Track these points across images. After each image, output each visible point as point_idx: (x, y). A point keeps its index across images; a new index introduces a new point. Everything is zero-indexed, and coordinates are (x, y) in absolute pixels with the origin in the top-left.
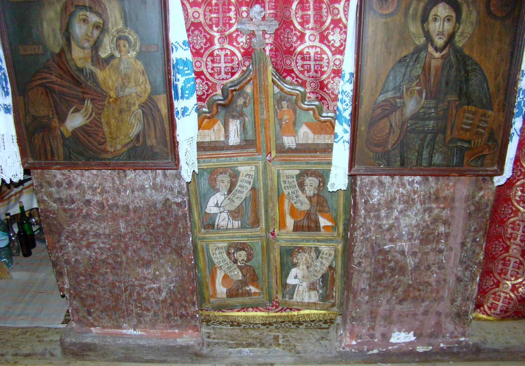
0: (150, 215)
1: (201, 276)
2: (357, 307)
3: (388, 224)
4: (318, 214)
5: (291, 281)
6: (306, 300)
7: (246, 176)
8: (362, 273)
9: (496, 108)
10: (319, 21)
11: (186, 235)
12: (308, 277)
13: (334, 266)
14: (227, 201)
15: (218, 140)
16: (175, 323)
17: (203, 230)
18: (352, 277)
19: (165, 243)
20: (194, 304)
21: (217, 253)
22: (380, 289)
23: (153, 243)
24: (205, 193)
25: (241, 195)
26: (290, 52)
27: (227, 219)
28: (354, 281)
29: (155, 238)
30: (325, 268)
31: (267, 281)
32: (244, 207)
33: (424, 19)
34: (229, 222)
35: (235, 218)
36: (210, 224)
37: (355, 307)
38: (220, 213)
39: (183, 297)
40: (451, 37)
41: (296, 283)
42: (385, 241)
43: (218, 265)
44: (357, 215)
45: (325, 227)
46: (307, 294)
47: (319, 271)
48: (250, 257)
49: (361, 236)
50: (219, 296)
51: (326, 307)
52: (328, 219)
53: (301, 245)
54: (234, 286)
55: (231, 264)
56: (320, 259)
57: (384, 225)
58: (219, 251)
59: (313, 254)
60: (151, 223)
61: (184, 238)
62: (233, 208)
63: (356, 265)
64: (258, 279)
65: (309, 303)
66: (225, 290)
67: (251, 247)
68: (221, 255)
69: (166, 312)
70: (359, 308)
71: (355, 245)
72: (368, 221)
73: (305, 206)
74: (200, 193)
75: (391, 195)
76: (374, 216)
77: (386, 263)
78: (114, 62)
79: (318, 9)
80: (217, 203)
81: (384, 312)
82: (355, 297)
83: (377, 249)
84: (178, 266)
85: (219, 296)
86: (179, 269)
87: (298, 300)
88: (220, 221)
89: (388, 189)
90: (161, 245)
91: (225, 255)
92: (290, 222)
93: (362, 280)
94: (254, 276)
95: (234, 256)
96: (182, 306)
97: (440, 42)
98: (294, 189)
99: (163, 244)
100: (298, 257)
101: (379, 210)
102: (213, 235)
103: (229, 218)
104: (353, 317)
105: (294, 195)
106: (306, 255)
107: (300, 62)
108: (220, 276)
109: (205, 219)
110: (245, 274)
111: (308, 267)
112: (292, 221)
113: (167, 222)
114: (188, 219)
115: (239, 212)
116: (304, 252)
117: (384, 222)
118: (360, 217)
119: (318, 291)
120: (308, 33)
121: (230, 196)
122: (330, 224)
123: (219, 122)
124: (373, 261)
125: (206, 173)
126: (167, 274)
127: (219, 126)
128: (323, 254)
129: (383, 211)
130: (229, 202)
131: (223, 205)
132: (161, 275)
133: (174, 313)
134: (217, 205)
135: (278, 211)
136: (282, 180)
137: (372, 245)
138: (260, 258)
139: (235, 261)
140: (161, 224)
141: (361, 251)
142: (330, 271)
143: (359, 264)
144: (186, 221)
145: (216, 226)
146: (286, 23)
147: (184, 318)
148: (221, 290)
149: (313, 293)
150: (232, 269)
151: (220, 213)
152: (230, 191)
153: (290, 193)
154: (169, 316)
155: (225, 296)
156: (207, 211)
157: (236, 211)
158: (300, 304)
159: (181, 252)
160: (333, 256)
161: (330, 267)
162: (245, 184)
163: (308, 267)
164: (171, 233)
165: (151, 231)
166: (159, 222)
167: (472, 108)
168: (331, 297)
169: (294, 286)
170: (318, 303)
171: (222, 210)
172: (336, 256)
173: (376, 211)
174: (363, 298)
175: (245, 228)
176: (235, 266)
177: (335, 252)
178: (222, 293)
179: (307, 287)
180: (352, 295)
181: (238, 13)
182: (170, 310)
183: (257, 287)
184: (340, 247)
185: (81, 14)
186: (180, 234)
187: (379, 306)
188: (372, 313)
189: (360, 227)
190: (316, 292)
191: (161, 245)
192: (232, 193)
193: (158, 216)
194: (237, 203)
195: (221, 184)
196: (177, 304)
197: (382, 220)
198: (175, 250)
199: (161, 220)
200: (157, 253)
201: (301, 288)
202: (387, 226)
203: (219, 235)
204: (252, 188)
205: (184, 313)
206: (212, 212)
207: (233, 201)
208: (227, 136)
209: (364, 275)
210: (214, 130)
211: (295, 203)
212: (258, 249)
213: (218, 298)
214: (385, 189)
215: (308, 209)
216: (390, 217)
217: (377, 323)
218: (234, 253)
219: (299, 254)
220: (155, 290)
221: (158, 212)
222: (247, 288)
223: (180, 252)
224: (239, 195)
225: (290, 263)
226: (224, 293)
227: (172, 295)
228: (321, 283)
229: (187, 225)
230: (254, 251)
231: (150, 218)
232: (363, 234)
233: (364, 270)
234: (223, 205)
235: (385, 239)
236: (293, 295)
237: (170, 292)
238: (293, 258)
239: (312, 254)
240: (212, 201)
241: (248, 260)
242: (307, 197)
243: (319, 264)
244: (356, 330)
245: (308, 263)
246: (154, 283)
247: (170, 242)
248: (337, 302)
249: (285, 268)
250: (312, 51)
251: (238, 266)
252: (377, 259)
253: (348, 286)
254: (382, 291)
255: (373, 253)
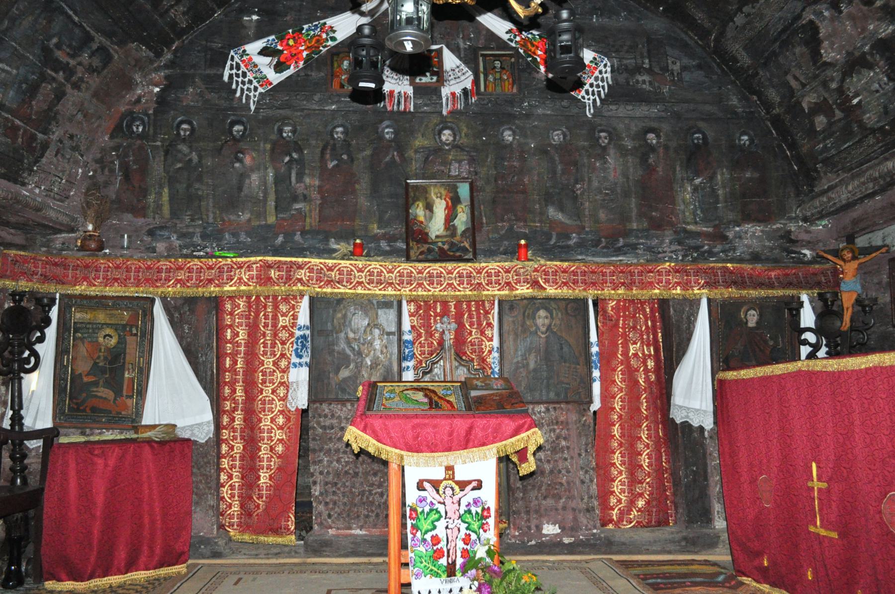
9: (581, 364)
10: (480, 324)
26: (464, 342)
40: (550, 326)
79: (479, 317)
82: (513, 494)
97: (544, 329)
107: (470, 347)
120: (474, 331)
146: (461, 325)
167: (567, 365)
181: (435, 321)
244: (517, 522)
250: (476, 341)
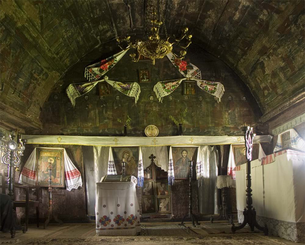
5: (160, 206)
33: (182, 153)
35: (149, 193)
52: (167, 192)
66: (147, 209)
73: (162, 190)
78: (131, 161)
91: (147, 201)
122: (167, 193)
139: (149, 202)
149: (165, 209)
169: (161, 208)
185: (126, 154)
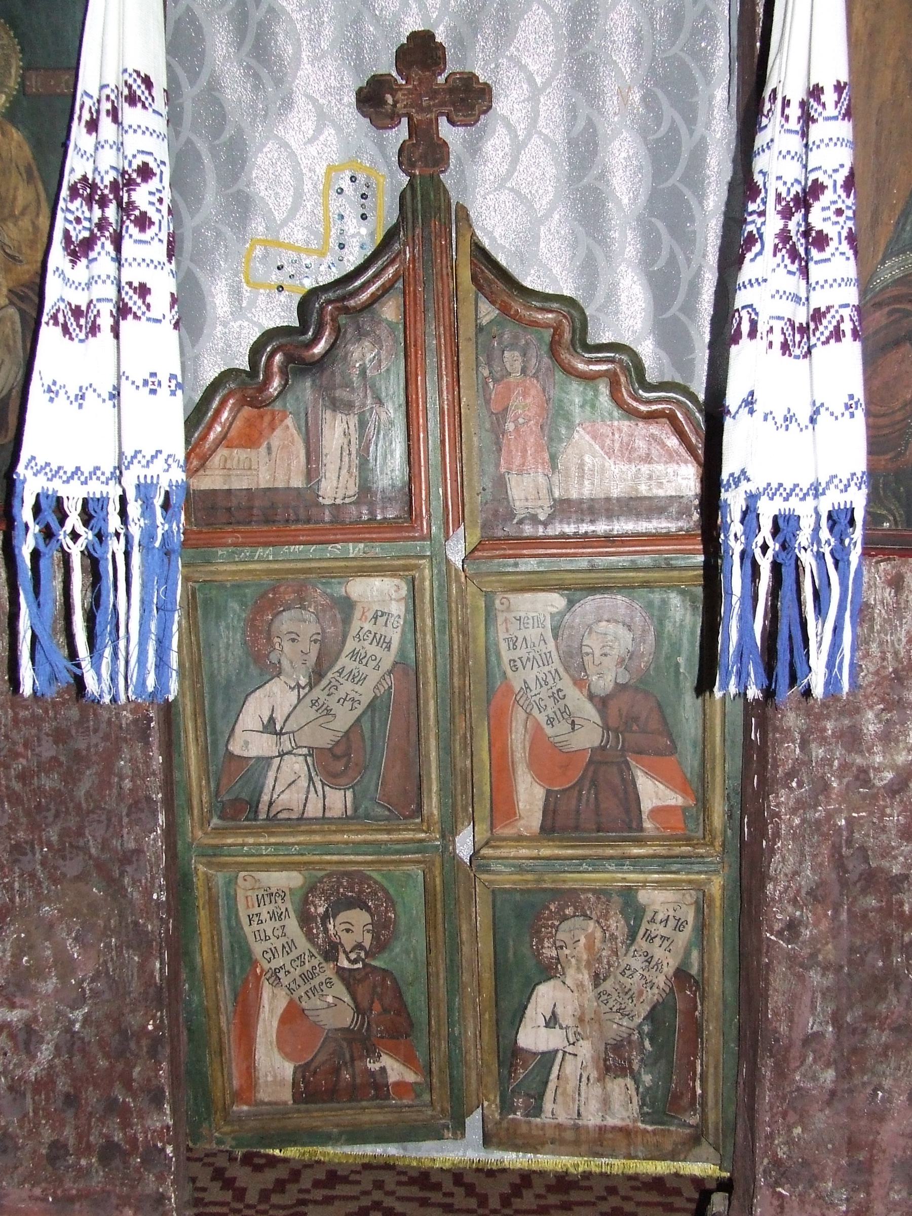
0: (16, 720)
1: (201, 1003)
2: (792, 1117)
3: (894, 767)
4: (633, 763)
5: (533, 1037)
6: (592, 1119)
7: (375, 618)
8: (807, 968)
11: (144, 805)
12: (597, 1019)
13: (694, 971)
14: (307, 713)
15: (280, 485)
16: (81, 1185)
17: (215, 821)
18: (768, 984)
19: (64, 833)
20: (157, 1099)
21: (265, 916)
22: (878, 1037)
23: (21, 834)
24: (229, 681)
25: (357, 688)
27: (303, 782)
28: (776, 1000)
29: (28, 813)
30: (661, 980)
31: (444, 1032)
32: (367, 735)
34: (312, 795)
35: (332, 778)
36: (240, 800)
37: (784, 1115)
38: (281, 755)
39: (120, 1066)
41: (551, 1046)
42: (883, 837)
43: (266, 966)
44: (776, 729)
45: (656, 812)
46: (596, 1090)
47: (641, 993)
48: (383, 933)
49: (794, 811)
50: (263, 1095)
51: (669, 1147)
52: (668, 782)
53: (572, 880)
54: (322, 1058)
55: (315, 962)
56: (641, 943)
57: (878, 770)
58: (271, 908)
59: (617, 924)
60: (17, 755)
61: (133, 816)
62: (325, 739)
63: (780, 934)
64: (411, 1025)
65: (602, 1130)
66: (287, 1069)
67: (386, 892)
68: (278, 924)
69: (47, 1134)
70: (801, 1121)
71: (772, 852)
72: (818, 752)
74: (212, 677)
75: (896, 653)
76: (840, 735)
77: (893, 926)
80: (272, 720)
81: (901, 1142)
82: (781, 1073)
83: (855, 867)
84: (106, 933)
85: (263, 1095)
86: (108, 946)
87: (562, 1118)
88: (278, 789)
89: (883, 630)
90: (49, 845)
91: (292, 924)
92: (530, 796)
93: (806, 999)
94: (398, 1013)
95: (326, 930)
96: (112, 1107)
98: (546, 669)
99: (55, 838)
100: (561, 936)
101: (858, 710)
102: (251, 840)
103: (311, 779)
104: (777, 1163)
105: (544, 693)
106: (592, 924)
108: (272, 1011)
109: (224, 781)
110: (365, 1004)
111: (597, 975)
112: (539, 793)
113: (77, 752)
114: (154, 740)
115: (347, 754)
116: (585, 915)
117: (878, 759)
118: (787, 734)
119: (637, 1081)
121: (317, 692)
122: (675, 799)
123: (289, 421)
124: (844, 916)
125: (234, 605)
126: (65, 966)
127: (286, 435)
128: (653, 920)
129: (870, 715)
130: (312, 714)
131: (292, 725)
132: (39, 972)
133: (80, 1137)
134: (269, 727)
135: (485, 756)
136: (502, 635)
137: (836, 849)
138: (419, 940)
139: (331, 952)
140: (54, 759)
141: (796, 873)
142: (682, 990)
143: (793, 927)
144: (147, 745)
145: (263, 807)
147: (117, 1162)
148: (275, 1069)
149: (619, 1087)
150: (315, 982)
151: (281, 755)
152: (318, 674)
153: (532, 685)
154: (57, 1150)
155: (286, 1095)
156: (236, 748)
157: (338, 751)
158: (569, 1135)
159: (122, 874)
160: (689, 927)
161: (681, 975)
162: (373, 649)
163: (597, 980)
164: (88, 795)
165: (17, 786)
166: (48, 750)
168: (685, 1101)
169: (548, 1058)
170: (637, 1131)
171: (287, 747)
172: (702, 927)
173: (842, 713)
174: (814, 1078)
175: (367, 817)
176: (329, 970)
177: (699, 911)
178: (278, 1083)
179: (596, 1060)
180: (770, 1062)
182: (63, 1125)
183: (408, 1060)
184: (716, 886)
186: (121, 797)
187: (879, 1116)
188: (852, 1145)
189: (790, 775)
190: (629, 1081)
191: (49, 845)
192: (324, 682)
193: (46, 727)
194: (344, 719)
195: (287, 646)
196: (92, 1097)
197: (869, 750)
198: (100, 866)
199: (56, 742)
200: (33, 875)
201: (571, 1068)
202: (889, 775)
203: (273, 840)
204: (395, 663)
205: (118, 1137)
206: (253, 752)
207: (328, 711)
208: (312, 472)
209: (815, 977)
210: (269, 448)
211: (550, 721)
212: (412, 902)
213: (263, 1103)
214: (871, 628)
215: (596, 744)
216: (897, 741)
217: (877, 1192)
218: (325, 917)
219: (565, 925)
220: (12, 1036)
221: (46, 711)
222: (373, 1066)
223: (116, 874)
224: (347, 687)
225: (531, 963)
226: (282, 1083)
227: (77, 1058)
228: (647, 1043)
229: (147, 764)
230: (399, 909)
231: (14, 734)
232: (800, 806)
233: (813, 955)
234: (292, 725)
235: (884, 829)
236: (541, 1096)
237: (71, 1044)
238: (541, 941)
239: (612, 923)
240: (253, 713)
241: (380, 946)
242: (591, 697)
243: (637, 963)
245: (599, 960)
246: (12, 1006)
247: (80, 833)
248: (712, 1117)
249: (515, 980)
251: (340, 971)
252: (856, 909)
253: (751, 1033)
254: (887, 1047)
255: (844, 883)
